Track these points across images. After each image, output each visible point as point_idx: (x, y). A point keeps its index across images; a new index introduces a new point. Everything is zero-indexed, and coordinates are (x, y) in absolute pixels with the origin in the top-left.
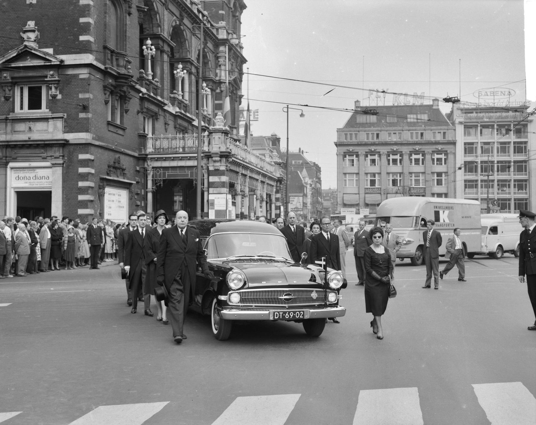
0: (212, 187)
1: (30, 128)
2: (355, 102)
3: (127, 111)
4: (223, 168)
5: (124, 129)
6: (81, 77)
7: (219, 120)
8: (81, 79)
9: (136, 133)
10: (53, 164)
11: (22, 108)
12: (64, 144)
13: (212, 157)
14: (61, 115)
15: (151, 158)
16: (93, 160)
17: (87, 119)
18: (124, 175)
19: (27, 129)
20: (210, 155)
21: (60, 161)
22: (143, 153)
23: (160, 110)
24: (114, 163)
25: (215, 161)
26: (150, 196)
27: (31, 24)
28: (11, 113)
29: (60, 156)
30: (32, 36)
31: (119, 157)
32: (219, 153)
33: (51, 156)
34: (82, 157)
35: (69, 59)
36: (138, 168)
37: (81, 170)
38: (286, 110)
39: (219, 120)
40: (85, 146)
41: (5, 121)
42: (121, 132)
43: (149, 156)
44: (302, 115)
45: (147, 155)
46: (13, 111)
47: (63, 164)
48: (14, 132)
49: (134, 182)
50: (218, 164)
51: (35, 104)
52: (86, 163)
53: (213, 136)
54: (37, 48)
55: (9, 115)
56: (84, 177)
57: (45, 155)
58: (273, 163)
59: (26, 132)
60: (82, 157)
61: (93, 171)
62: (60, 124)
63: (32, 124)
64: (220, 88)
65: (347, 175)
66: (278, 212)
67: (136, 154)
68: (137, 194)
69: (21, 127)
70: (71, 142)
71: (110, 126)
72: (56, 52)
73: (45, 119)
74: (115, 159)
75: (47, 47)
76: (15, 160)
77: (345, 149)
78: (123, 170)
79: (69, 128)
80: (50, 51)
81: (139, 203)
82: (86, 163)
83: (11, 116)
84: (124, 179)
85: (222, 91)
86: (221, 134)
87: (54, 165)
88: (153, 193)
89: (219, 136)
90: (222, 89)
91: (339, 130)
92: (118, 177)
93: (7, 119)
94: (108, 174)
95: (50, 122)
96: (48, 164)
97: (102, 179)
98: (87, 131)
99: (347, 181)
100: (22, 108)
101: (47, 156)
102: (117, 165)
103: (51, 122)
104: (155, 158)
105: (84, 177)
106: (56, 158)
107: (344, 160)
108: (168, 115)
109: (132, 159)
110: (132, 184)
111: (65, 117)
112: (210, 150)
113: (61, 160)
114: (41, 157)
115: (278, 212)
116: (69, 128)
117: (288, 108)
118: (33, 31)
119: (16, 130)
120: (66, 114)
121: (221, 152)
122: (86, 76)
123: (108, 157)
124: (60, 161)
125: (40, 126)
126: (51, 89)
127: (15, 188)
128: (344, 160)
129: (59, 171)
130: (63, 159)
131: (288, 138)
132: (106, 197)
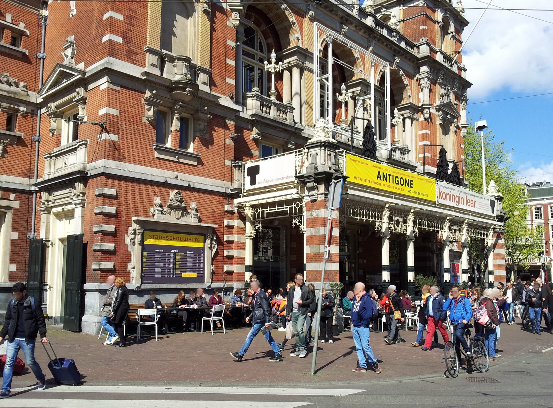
6: (102, 87)
12: (83, 177)
26: (249, 244)
27: (72, 38)
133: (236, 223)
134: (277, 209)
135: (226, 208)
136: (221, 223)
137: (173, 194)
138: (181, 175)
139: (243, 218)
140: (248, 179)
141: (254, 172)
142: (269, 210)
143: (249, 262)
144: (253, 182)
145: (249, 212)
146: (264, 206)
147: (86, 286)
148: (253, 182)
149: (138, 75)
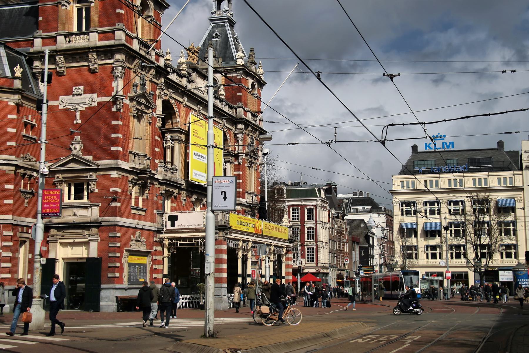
2: (412, 147)
6: (112, 176)
8: (112, 178)
11: (69, 199)
26: (166, 261)
30: (78, 147)
35: (103, 163)
51: (78, 195)
54: (81, 156)
72: (95, 158)
73: (85, 207)
75: (88, 155)
76: (63, 237)
80: (90, 158)
88: (168, 258)
100: (69, 199)
118: (79, 143)
122: (116, 176)
126: (90, 185)
133: (159, 248)
134: (187, 242)
135: (155, 239)
136: (152, 249)
137: (137, 233)
138: (140, 222)
139: (163, 246)
140: (169, 223)
141: (173, 219)
142: (181, 242)
143: (166, 272)
144: (173, 225)
145: (166, 242)
146: (178, 239)
147: (103, 286)
148: (173, 225)
149: (128, 169)
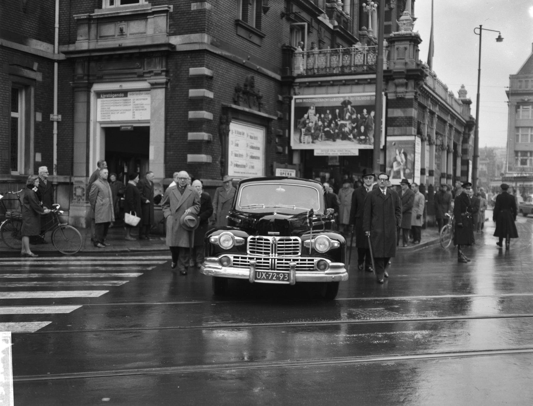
0: (391, 126)
1: (121, 30)
3: (266, 10)
4: (410, 96)
5: (261, 37)
7: (405, 22)
9: (280, 45)
10: (152, 84)
13: (393, 79)
14: (164, 7)
15: (300, 83)
16: (211, 78)
17: (202, 12)
18: (260, 107)
19: (118, 32)
20: (391, 76)
21: (162, 79)
22: (288, 74)
23: (313, 21)
24: (246, 85)
25: (397, 86)
28: (96, 10)
29: (162, 71)
31: (253, 78)
32: (406, 72)
33: (150, 72)
34: (193, 71)
36: (280, 98)
37: (193, 93)
38: (478, 31)
39: (405, 22)
40: (197, 56)
41: (87, 22)
42: (256, 40)
43: (298, 80)
44: (499, 39)
45: (295, 78)
46: (100, 7)
47: (166, 83)
48: (100, 37)
49: (275, 118)
50: (401, 89)
52: (200, 81)
53: (396, 46)
55: (93, 12)
56: (198, 103)
57: (141, 70)
58: (460, 102)
59: (116, 37)
60: (193, 71)
61: (210, 95)
62: (162, 22)
63: (123, 25)
64: (390, 4)
65: (520, 130)
66: (465, 168)
67: (278, 77)
68: (279, 136)
69: (110, 30)
70: (179, 48)
71: (239, 29)
73: (142, 16)
74: (247, 80)
76: (101, 80)
77: (519, 98)
78: (259, 98)
79: (176, 28)
81: (280, 149)
82: (200, 81)
83: (97, 13)
84: (260, 111)
85: (391, 9)
86: (408, 43)
87: (154, 86)
89: (405, 46)
90: (392, 6)
91: (512, 77)
92: (250, 107)
93: (90, 19)
94: (235, 103)
95: (149, 20)
96: (144, 85)
97: (226, 110)
98: (202, 31)
99: (520, 136)
101: (144, 73)
102: (248, 89)
103: (151, 20)
104: (305, 83)
105: (198, 103)
106: (157, 74)
107: (516, 112)
108: (323, 29)
109: (272, 83)
110: (272, 119)
111: (171, 10)
112: (391, 68)
113: (164, 77)
114: (135, 73)
115: (465, 168)
116: (176, 28)
117: (481, 29)
119: (102, 35)
120: (172, 6)
121: (408, 71)
123: (234, 76)
124: (162, 79)
125: (135, 27)
127: (101, 123)
128: (516, 112)
129: (160, 94)
130: (166, 76)
131: (479, 70)
132: (232, 137)
